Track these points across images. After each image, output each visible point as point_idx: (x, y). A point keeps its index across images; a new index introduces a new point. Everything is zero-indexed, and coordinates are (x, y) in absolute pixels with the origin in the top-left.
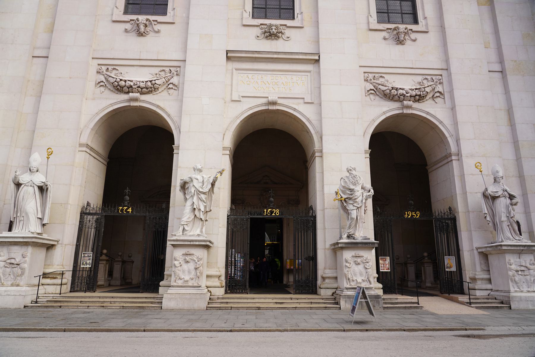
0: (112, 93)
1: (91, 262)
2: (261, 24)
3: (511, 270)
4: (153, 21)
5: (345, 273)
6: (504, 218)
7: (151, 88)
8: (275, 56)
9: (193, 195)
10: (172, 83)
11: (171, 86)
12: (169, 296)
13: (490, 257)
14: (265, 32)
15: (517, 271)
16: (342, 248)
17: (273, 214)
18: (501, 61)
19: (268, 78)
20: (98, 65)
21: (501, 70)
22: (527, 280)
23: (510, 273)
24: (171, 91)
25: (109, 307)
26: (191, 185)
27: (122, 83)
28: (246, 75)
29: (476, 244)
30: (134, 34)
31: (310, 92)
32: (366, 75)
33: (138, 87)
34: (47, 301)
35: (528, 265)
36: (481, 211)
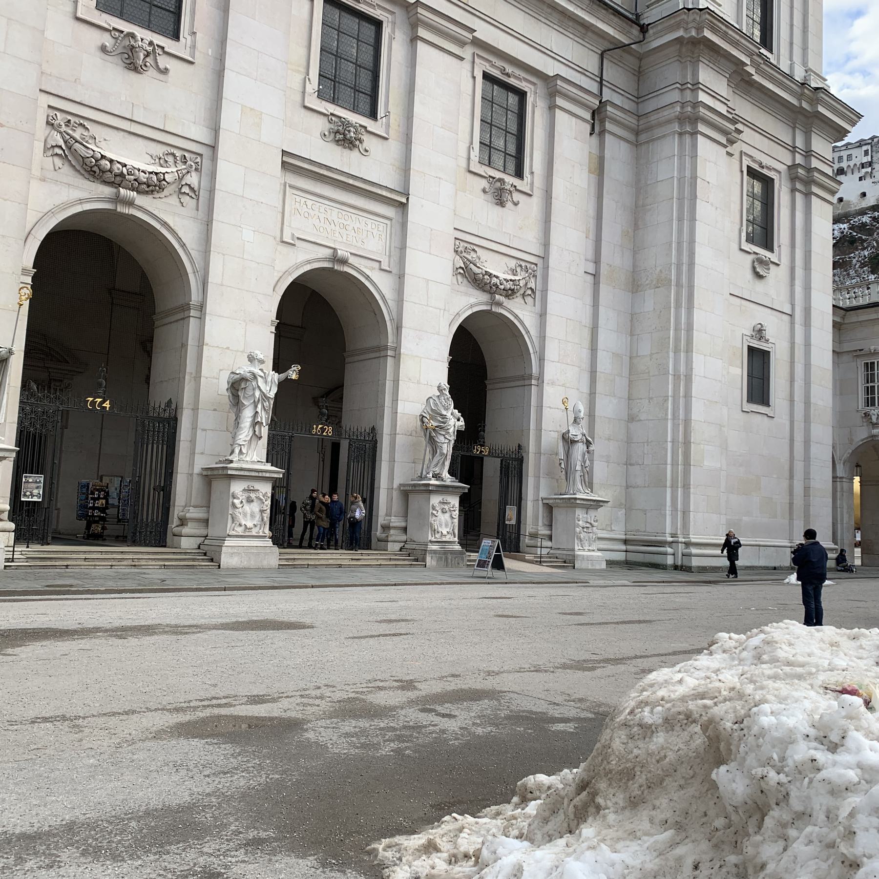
0: (77, 174)
1: (41, 493)
2: (332, 114)
3: (578, 526)
4: (158, 45)
5: (431, 523)
6: (578, 468)
7: (155, 186)
8: (351, 182)
9: (256, 400)
10: (189, 185)
11: (186, 189)
12: (230, 550)
13: (555, 511)
14: (338, 132)
15: (583, 528)
16: (430, 492)
17: (324, 434)
18: (597, 261)
19: (334, 213)
20: (49, 106)
21: (594, 273)
22: (589, 538)
23: (578, 530)
24: (185, 199)
25: (143, 567)
26: (254, 383)
27: (105, 164)
28: (303, 200)
29: (543, 494)
30: (117, 59)
31: (387, 254)
32: (457, 242)
33: (135, 180)
34: (28, 558)
35: (592, 522)
36: (557, 454)
